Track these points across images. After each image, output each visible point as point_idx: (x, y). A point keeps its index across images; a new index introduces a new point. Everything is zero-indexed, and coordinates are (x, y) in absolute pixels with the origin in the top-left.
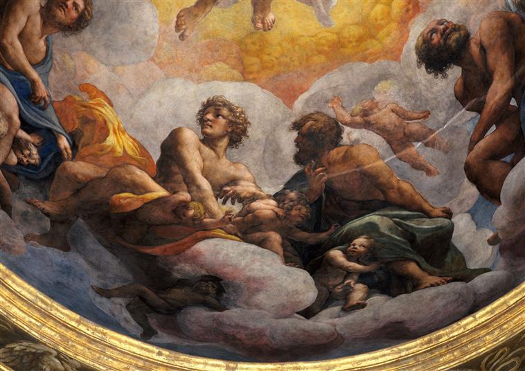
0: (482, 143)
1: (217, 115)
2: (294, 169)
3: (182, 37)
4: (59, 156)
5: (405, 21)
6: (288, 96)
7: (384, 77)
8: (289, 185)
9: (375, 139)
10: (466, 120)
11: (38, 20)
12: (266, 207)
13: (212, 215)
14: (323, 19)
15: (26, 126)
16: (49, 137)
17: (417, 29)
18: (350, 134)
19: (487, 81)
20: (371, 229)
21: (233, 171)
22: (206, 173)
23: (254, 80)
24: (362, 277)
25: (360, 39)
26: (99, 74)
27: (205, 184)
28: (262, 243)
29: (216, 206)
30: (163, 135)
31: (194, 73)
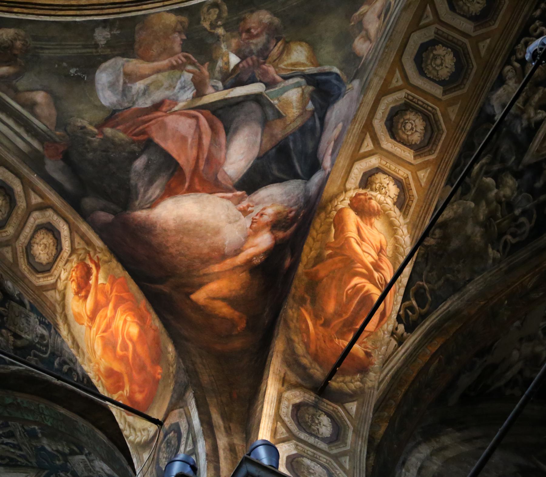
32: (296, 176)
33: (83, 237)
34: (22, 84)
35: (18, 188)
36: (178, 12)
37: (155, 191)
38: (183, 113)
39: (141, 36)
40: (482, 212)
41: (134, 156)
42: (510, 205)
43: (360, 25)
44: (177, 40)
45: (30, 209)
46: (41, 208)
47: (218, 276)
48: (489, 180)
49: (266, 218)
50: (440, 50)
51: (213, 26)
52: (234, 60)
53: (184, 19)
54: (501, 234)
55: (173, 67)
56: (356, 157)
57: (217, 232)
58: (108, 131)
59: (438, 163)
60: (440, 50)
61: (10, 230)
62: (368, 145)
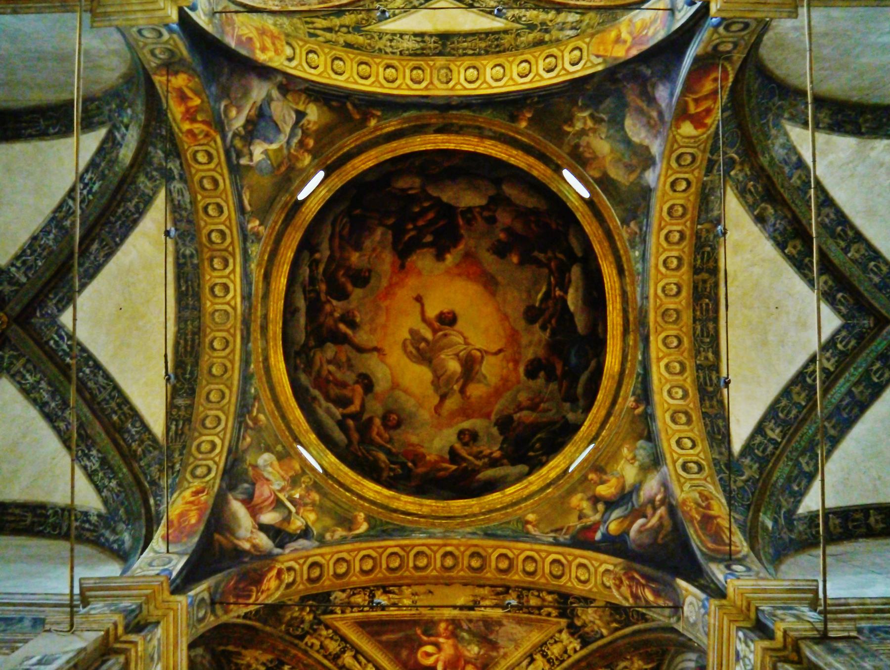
0: (564, 388)
1: (465, 435)
2: (501, 438)
3: (439, 415)
4: (410, 470)
5: (516, 369)
6: (488, 416)
7: (518, 391)
8: (502, 443)
9: (525, 413)
10: (553, 386)
11: (382, 428)
12: (497, 454)
13: (478, 466)
14: (488, 385)
15: (392, 463)
16: (403, 465)
17: (521, 369)
18: (516, 416)
19: (554, 369)
20: (539, 440)
21: (479, 449)
22: (470, 454)
23: (473, 417)
24: (542, 455)
25: (504, 384)
26: (414, 439)
27: (470, 458)
28: (502, 465)
29: (479, 463)
30: (447, 449)
31: (450, 425)
32: (274, 542)
33: (214, 483)
34: (249, 431)
35: (218, 450)
36: (301, 468)
37: (241, 497)
38: (270, 489)
39: (286, 461)
40: (296, 614)
41: (246, 482)
42: (303, 622)
43: (334, 531)
44: (292, 473)
45: (212, 459)
46: (215, 463)
47: (226, 538)
48: (308, 609)
49: (254, 541)
50: (345, 565)
51: (304, 482)
52: (297, 496)
53: (300, 472)
54: (291, 626)
55: (282, 477)
56: (295, 560)
57: (240, 526)
58: (250, 468)
59: (307, 589)
60: (345, 565)
61: (200, 456)
62: (301, 561)
